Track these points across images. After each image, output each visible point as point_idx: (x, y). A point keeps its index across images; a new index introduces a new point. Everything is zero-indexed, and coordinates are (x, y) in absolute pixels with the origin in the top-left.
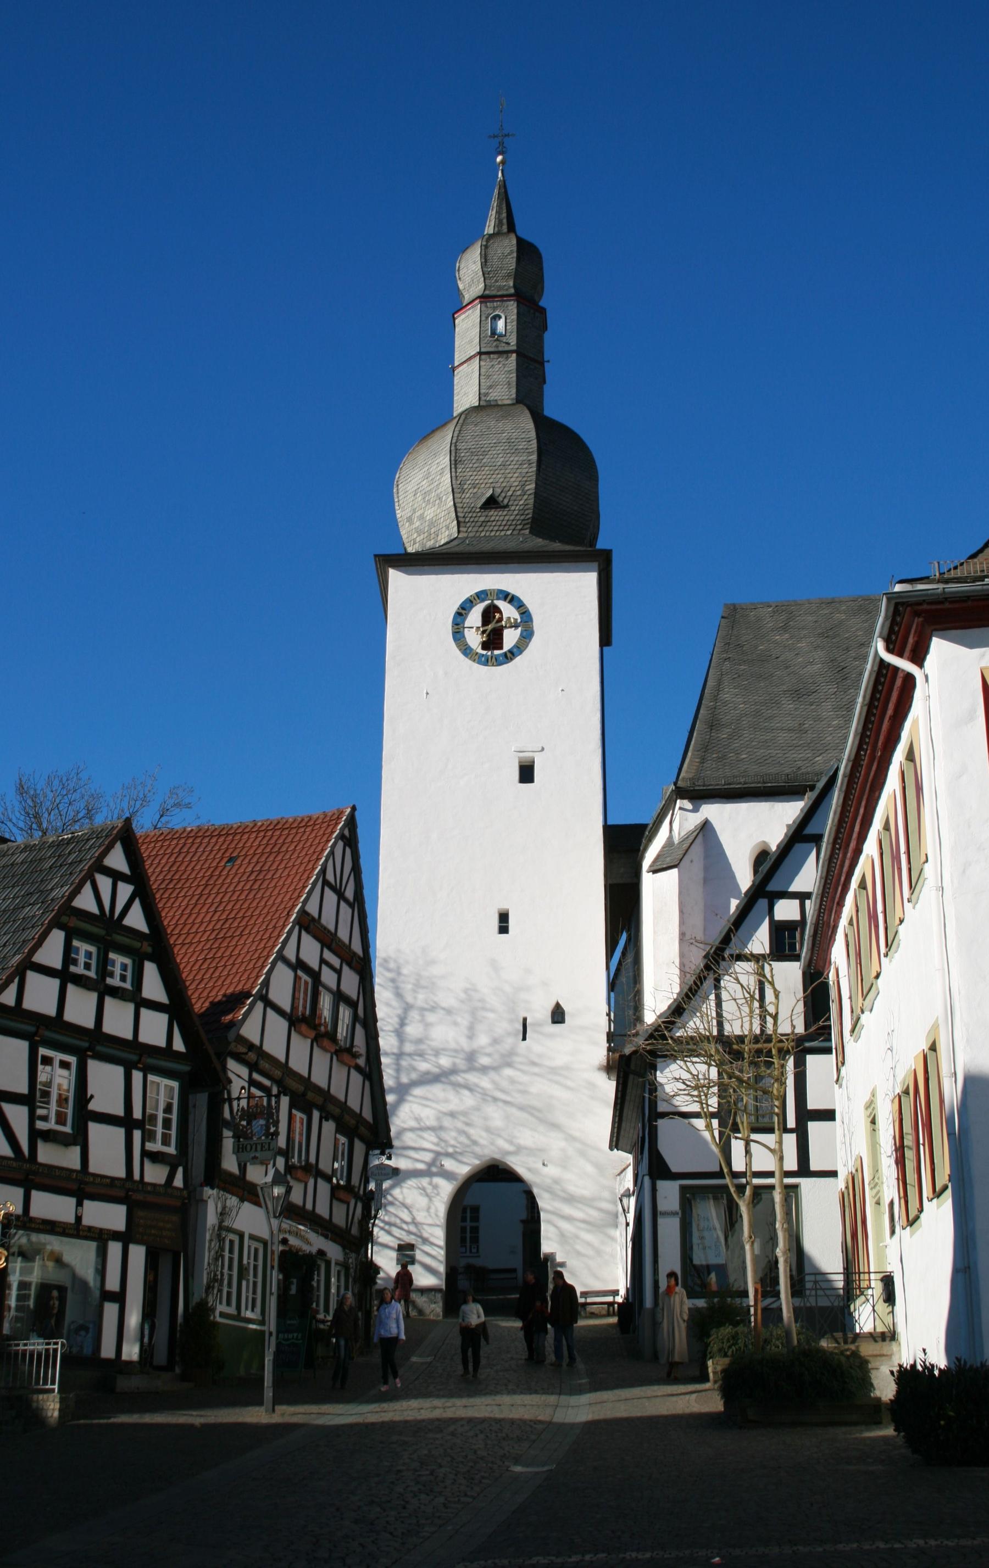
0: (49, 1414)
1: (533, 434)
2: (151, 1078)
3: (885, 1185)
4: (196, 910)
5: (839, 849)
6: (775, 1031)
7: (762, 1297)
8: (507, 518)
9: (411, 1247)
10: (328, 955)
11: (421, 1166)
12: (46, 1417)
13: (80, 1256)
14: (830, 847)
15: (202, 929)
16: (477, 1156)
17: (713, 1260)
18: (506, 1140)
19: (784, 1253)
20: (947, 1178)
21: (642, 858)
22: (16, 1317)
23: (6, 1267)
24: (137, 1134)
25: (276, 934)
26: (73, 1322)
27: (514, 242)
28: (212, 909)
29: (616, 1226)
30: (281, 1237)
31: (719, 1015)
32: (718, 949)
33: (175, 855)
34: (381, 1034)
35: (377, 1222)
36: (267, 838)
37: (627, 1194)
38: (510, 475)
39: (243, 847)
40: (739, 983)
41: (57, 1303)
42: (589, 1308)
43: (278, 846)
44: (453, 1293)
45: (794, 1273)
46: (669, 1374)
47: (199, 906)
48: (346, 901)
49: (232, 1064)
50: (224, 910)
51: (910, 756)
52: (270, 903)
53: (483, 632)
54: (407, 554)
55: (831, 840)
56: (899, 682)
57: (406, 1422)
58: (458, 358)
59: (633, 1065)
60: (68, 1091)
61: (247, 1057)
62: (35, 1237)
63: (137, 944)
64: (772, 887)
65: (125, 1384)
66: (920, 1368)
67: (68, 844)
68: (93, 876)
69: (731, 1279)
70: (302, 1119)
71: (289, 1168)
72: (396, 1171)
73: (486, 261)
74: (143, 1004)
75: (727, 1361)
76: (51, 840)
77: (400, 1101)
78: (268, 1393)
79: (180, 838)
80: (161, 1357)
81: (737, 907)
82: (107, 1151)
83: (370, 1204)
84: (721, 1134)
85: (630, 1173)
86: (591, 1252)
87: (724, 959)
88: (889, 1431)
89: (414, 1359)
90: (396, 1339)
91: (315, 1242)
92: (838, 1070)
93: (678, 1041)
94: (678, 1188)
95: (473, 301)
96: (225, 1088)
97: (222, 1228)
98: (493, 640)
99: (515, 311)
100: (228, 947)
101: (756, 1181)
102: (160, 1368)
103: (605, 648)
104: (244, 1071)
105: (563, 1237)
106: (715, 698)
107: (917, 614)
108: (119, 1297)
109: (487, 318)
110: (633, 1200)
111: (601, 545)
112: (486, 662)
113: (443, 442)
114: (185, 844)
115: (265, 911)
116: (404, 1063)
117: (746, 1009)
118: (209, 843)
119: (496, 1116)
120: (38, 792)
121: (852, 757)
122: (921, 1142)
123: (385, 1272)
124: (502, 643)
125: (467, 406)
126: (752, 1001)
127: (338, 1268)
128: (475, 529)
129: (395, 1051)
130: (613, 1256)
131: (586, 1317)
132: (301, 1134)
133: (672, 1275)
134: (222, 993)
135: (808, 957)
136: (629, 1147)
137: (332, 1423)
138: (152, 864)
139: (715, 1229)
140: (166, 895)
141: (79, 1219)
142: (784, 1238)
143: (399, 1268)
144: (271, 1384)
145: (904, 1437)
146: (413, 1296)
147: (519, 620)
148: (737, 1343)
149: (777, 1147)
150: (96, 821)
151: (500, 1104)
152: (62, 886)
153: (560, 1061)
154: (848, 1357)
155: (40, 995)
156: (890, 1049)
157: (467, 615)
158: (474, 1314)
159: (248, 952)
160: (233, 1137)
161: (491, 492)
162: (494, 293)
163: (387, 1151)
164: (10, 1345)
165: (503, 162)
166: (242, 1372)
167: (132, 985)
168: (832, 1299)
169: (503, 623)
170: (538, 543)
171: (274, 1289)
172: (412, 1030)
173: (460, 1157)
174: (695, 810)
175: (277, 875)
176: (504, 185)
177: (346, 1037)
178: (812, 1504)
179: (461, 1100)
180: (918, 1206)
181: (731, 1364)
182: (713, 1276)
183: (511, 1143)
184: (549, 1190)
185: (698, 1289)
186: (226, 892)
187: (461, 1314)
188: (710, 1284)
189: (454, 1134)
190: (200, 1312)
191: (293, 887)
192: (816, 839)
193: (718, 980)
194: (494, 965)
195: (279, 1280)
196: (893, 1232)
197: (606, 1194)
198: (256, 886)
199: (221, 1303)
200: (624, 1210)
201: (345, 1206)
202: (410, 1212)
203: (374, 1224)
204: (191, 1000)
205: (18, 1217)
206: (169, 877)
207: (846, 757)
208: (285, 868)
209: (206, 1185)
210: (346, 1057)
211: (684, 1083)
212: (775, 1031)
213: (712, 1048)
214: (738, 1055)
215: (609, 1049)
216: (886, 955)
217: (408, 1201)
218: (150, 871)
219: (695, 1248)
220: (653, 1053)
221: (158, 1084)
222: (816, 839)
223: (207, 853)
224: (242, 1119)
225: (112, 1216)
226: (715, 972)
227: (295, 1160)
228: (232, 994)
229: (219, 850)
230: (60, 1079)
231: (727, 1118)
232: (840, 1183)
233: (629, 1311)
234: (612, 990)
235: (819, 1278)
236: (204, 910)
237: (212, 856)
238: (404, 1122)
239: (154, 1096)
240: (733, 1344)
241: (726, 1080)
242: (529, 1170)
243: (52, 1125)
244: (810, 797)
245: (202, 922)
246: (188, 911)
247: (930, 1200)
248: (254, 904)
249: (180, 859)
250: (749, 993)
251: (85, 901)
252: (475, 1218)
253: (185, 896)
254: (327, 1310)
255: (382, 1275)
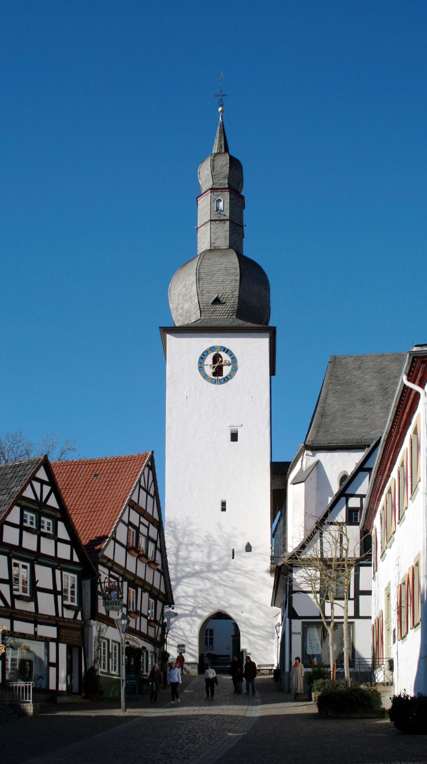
0: (29, 711)
1: (237, 265)
2: (64, 573)
3: (392, 623)
4: (80, 499)
5: (380, 475)
6: (347, 556)
7: (336, 667)
8: (224, 309)
9: (183, 646)
10: (143, 520)
11: (187, 612)
12: (28, 712)
13: (38, 648)
14: (375, 474)
15: (84, 507)
16: (212, 608)
17: (315, 653)
18: (225, 602)
19: (347, 650)
20: (419, 620)
21: (288, 477)
22: (11, 673)
23: (5, 652)
24: (59, 597)
25: (118, 510)
26: (36, 675)
27: (228, 158)
28: (88, 498)
29: (273, 638)
30: (126, 641)
31: (322, 549)
32: (322, 519)
33: (69, 473)
34: (168, 555)
35: (168, 635)
36: (112, 466)
37: (279, 625)
38: (226, 287)
39: (101, 470)
40: (331, 535)
41: (29, 667)
42: (261, 671)
43: (118, 469)
44: (202, 666)
45: (351, 658)
46: (295, 698)
47: (82, 497)
48: (151, 495)
49: (100, 568)
50: (93, 499)
51: (416, 432)
52: (115, 495)
53: (213, 367)
54: (175, 327)
55: (376, 471)
56: (412, 396)
57: (183, 716)
58: (200, 222)
59: (282, 573)
60: (27, 578)
61: (107, 565)
62: (17, 640)
63: (54, 514)
64: (348, 492)
65: (60, 700)
66: (402, 696)
67: (18, 467)
68: (31, 482)
69: (323, 660)
70: (133, 592)
71: (128, 613)
72: (176, 614)
73: (213, 169)
74: (58, 541)
75: (320, 693)
76: (10, 465)
77: (177, 584)
78: (123, 704)
79: (71, 465)
80: (76, 689)
81: (331, 501)
82: (46, 604)
83: (164, 628)
84: (321, 600)
85: (280, 616)
86: (262, 649)
87: (324, 524)
88: (388, 721)
89: (186, 691)
90: (177, 683)
91: (141, 643)
92: (374, 574)
93: (303, 560)
94: (301, 623)
95: (207, 191)
96: (98, 578)
97: (99, 637)
98: (218, 372)
99: (229, 197)
100: (96, 515)
101: (336, 620)
102: (75, 694)
103: (272, 377)
104: (106, 571)
105: (250, 643)
106: (324, 402)
107: (423, 362)
108: (56, 665)
109: (214, 201)
110: (281, 628)
111: (271, 324)
112: (215, 382)
113: (193, 266)
114: (74, 468)
115: (113, 499)
116: (179, 568)
117: (334, 546)
118: (85, 467)
119: (220, 591)
120: (2, 442)
121: (388, 432)
122: (409, 604)
123: (172, 656)
124: (222, 373)
125: (204, 249)
126: (337, 543)
127: (152, 654)
128: (209, 315)
129: (175, 563)
130: (272, 651)
131: (260, 675)
132: (133, 598)
133: (297, 658)
134: (94, 536)
135: (363, 524)
136: (279, 605)
137: (151, 716)
138: (58, 477)
139: (317, 640)
140: (66, 491)
141: (36, 633)
142: (347, 644)
143: (178, 654)
144: (124, 700)
145: (394, 723)
146: (185, 666)
147: (231, 362)
148: (325, 686)
149: (345, 606)
150: (31, 456)
151: (222, 586)
152: (17, 487)
153: (249, 568)
154: (372, 692)
155: (11, 536)
156: (398, 565)
157: (205, 358)
158: (211, 673)
159: (106, 518)
160: (103, 599)
161: (216, 296)
162: (218, 187)
163: (172, 606)
164: (9, 684)
165: (222, 111)
166: (111, 695)
167: (53, 532)
168: (366, 669)
169: (223, 363)
170: (240, 322)
171: (124, 662)
172: (182, 553)
173: (205, 609)
174: (314, 456)
175: (118, 483)
176: (223, 125)
177: (152, 557)
178: (354, 748)
179: (205, 584)
180: (406, 631)
181: (322, 694)
182: (315, 659)
183: (227, 603)
184: (244, 623)
185: (309, 664)
186: (94, 491)
187: (206, 673)
188: (314, 662)
189: (202, 599)
190: (92, 672)
191: (125, 489)
192: (369, 470)
193: (321, 534)
194: (220, 525)
195: (126, 659)
196: (394, 642)
197: (269, 625)
198: (108, 488)
199: (101, 668)
200: (277, 632)
201: (154, 629)
202: (183, 631)
203: (167, 636)
204: (80, 539)
205: (8, 632)
206: (67, 483)
207: (385, 432)
208: (121, 480)
209: (92, 619)
210: (152, 565)
211: (305, 578)
212: (347, 556)
213: (318, 563)
214: (329, 567)
215: (272, 563)
216: (399, 523)
217: (182, 627)
218: (58, 480)
219: (308, 647)
220: (291, 565)
221: (68, 576)
222: (369, 470)
223: (84, 472)
224: (106, 591)
225: (51, 632)
226: (320, 530)
227: (131, 609)
228: (99, 537)
229: (90, 471)
230: (22, 573)
231: (324, 594)
232: (373, 621)
233: (278, 673)
234: (273, 537)
235: (361, 660)
236: (84, 498)
237: (86, 474)
238: (179, 593)
239: (66, 581)
240: (323, 686)
241: (324, 577)
242: (235, 614)
243: (20, 593)
244: (368, 450)
245: (84, 504)
246: (77, 499)
247: (411, 629)
248: (107, 496)
249: (72, 474)
250: (335, 539)
251: (28, 493)
252: (212, 634)
253: (75, 492)
254: (147, 671)
255: (171, 657)
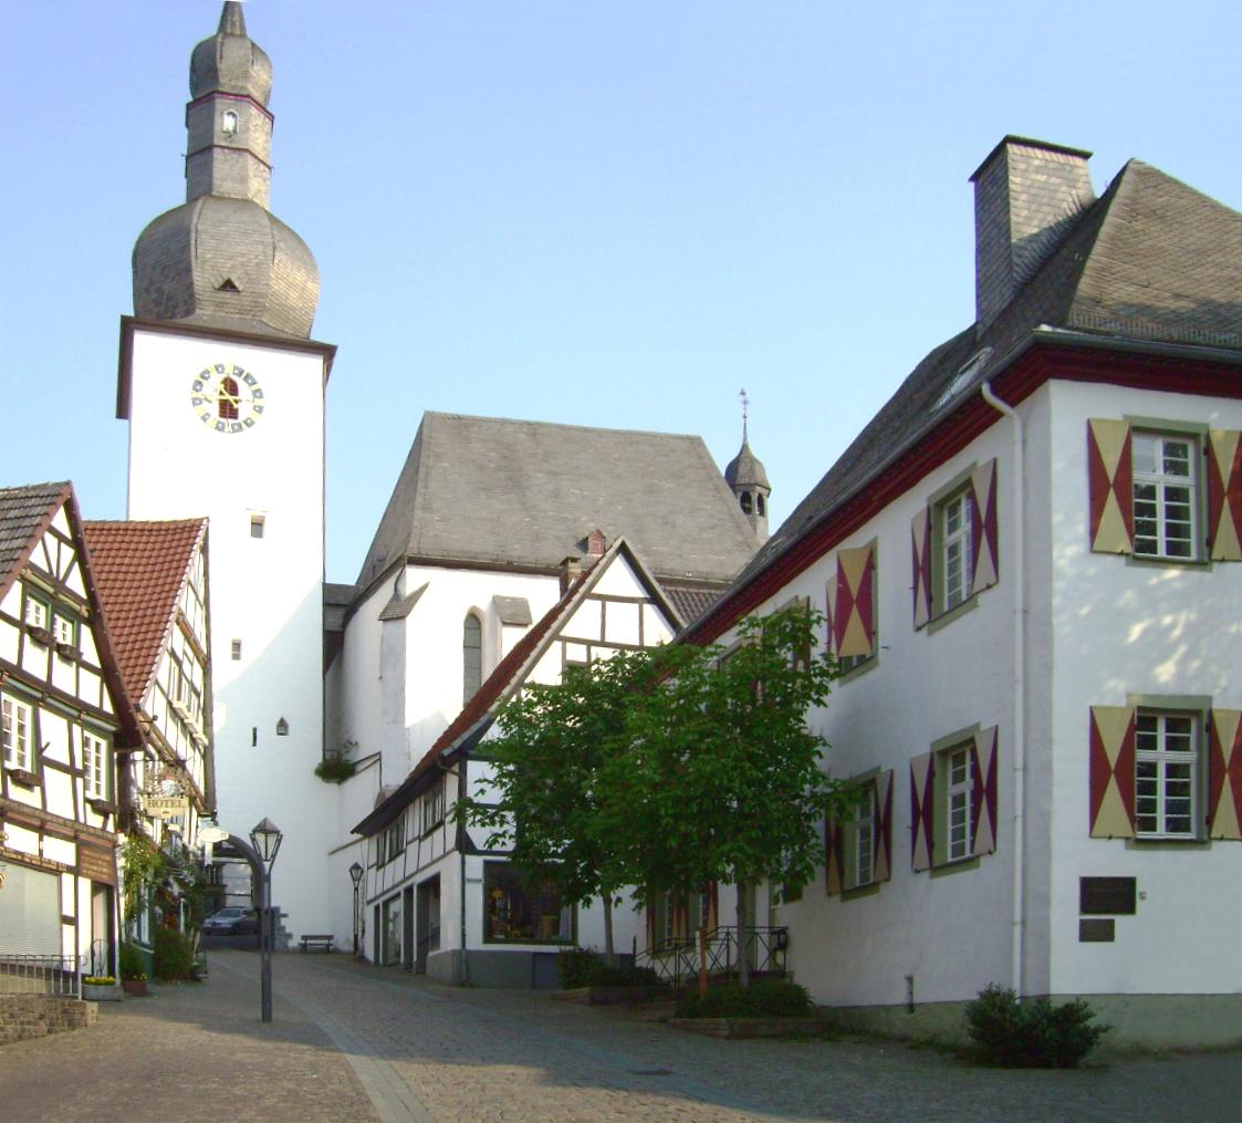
24: (79, 781)
108: (73, 921)
225: (61, 851)
